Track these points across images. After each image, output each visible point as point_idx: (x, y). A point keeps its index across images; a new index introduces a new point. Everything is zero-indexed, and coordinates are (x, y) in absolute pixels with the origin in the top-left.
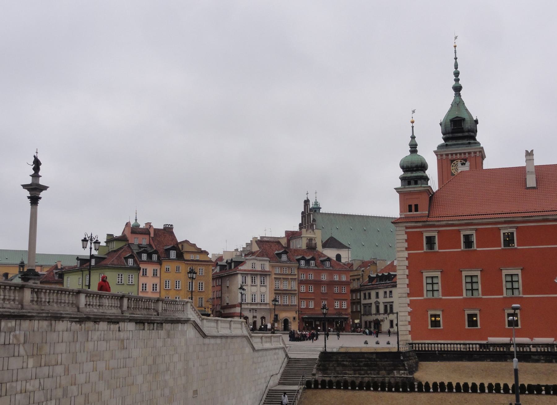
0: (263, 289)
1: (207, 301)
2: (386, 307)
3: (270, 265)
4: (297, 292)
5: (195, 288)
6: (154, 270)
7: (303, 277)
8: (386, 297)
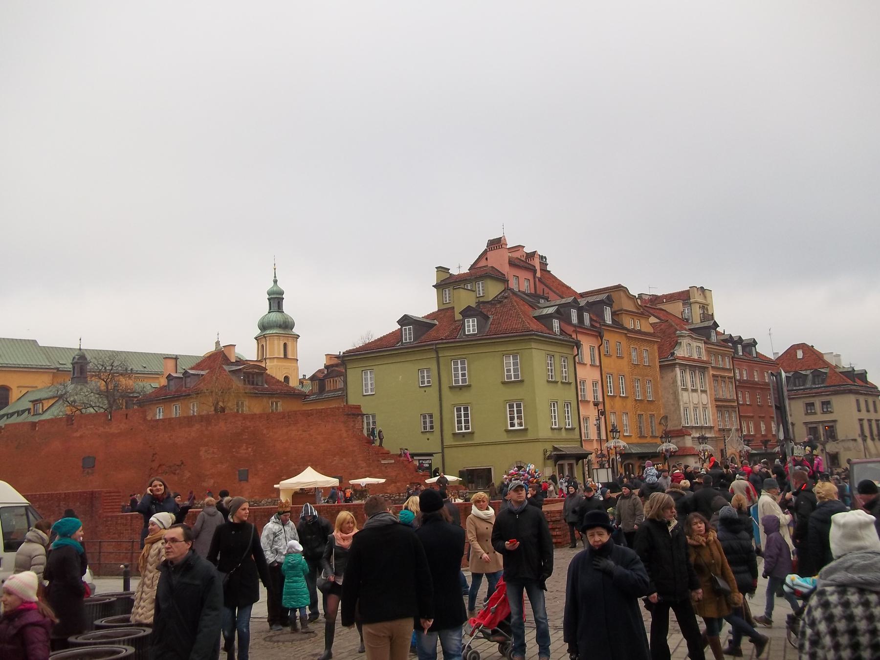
0: (705, 399)
2: (813, 430)
8: (815, 413)
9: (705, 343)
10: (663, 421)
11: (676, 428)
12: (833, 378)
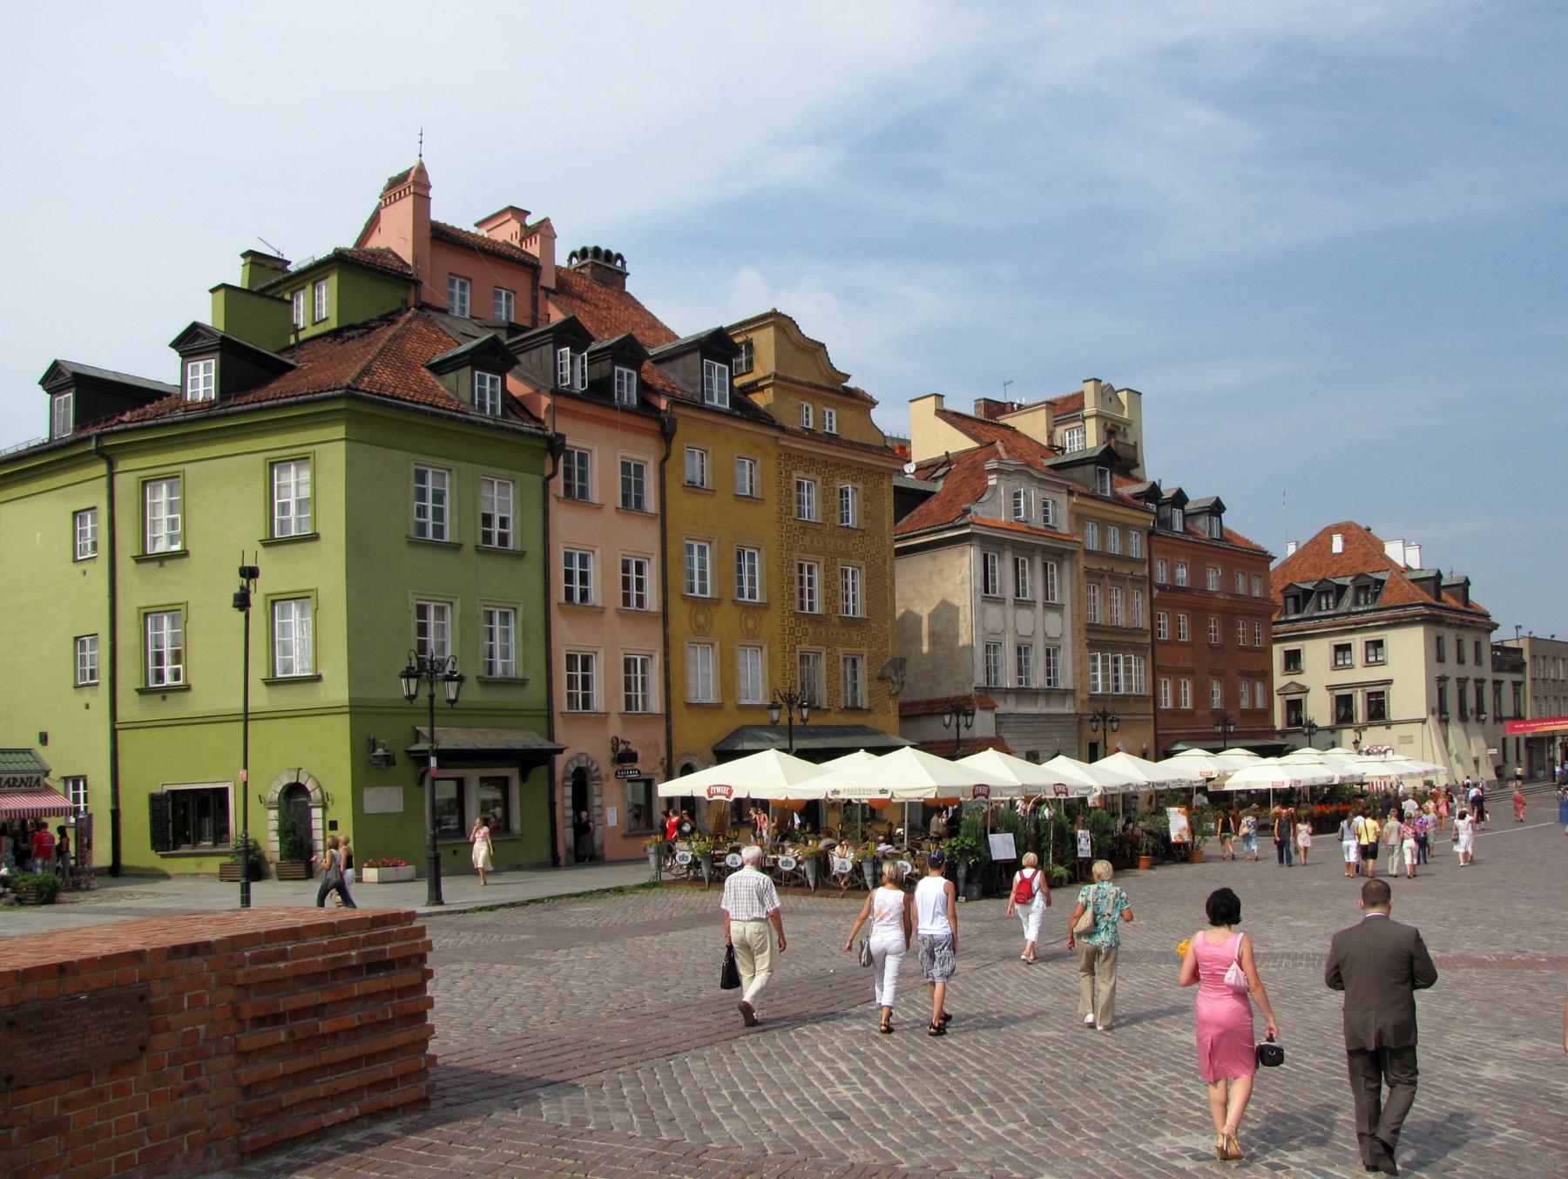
0: (1056, 625)
1: (881, 679)
2: (1343, 705)
3: (1071, 512)
4: (1148, 640)
5: (828, 601)
6: (625, 466)
7: (1162, 576)
8: (1351, 667)
9: (1071, 493)
10: (889, 672)
11: (960, 693)
12: (1396, 591)
